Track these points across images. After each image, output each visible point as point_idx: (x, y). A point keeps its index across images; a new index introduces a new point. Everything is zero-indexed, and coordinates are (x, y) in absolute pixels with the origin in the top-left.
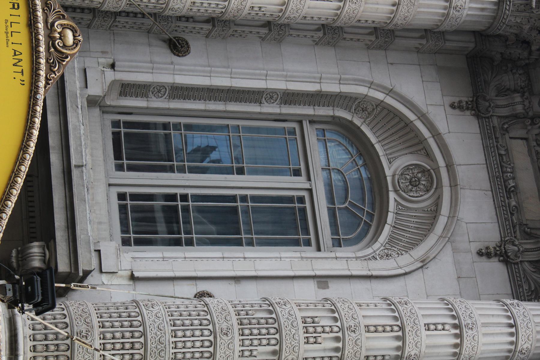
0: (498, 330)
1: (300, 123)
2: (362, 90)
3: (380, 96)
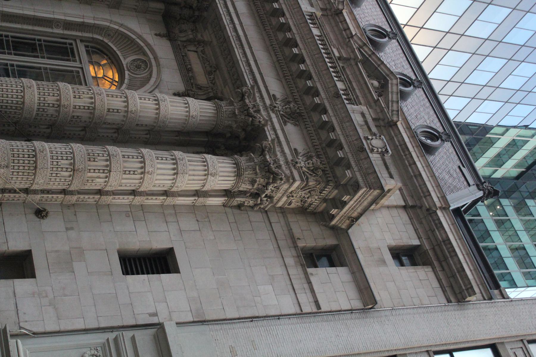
0: (178, 105)
1: (75, 40)
2: (108, 24)
3: (117, 27)
